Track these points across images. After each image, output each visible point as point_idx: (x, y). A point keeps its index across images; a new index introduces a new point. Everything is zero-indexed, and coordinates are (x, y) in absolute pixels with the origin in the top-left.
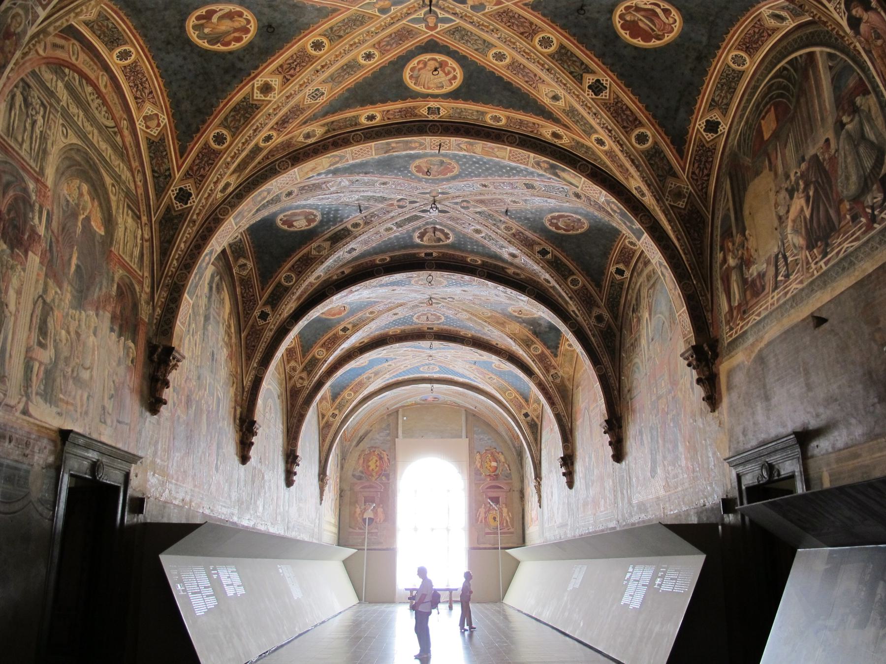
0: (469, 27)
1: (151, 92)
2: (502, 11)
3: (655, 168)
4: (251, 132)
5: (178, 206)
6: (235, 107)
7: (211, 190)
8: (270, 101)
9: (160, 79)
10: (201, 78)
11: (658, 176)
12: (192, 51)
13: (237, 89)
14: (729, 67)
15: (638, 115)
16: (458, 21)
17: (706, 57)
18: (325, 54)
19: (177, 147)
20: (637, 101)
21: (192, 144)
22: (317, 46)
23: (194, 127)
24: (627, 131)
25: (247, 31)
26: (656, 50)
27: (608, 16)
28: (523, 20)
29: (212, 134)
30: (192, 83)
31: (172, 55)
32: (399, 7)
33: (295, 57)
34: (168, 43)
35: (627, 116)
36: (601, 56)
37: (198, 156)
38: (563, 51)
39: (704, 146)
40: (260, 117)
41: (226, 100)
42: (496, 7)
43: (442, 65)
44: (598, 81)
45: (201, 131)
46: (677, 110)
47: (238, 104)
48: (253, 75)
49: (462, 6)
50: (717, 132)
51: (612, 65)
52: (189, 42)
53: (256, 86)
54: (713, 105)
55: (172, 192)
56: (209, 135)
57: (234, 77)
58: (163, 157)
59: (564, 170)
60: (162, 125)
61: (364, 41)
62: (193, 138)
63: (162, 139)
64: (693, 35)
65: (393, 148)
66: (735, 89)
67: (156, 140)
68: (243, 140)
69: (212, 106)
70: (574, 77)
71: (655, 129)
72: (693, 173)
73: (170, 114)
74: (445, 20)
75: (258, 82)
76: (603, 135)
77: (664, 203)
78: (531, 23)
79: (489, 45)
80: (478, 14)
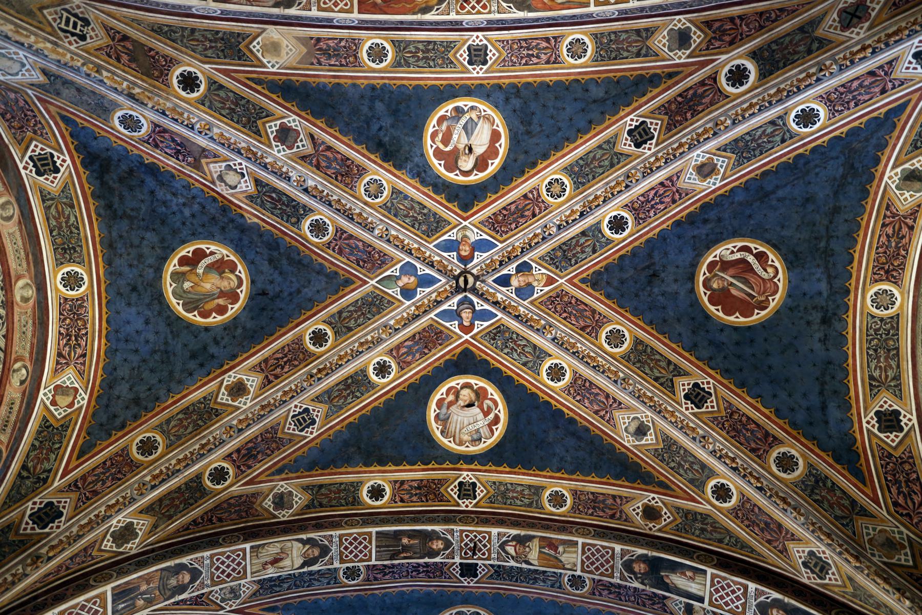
0: (514, 324)
2: (553, 294)
3: (826, 505)
4: (197, 447)
6: (188, 408)
7: (97, 516)
8: (238, 408)
9: (103, 341)
10: (157, 357)
11: (836, 518)
12: (160, 313)
13: (199, 384)
14: (873, 317)
15: (768, 428)
16: (500, 315)
17: (835, 314)
18: (327, 352)
19: (80, 442)
20: (759, 406)
21: (105, 443)
22: (319, 338)
23: (118, 422)
24: (759, 454)
25: (234, 298)
26: (764, 325)
27: (689, 285)
28: (582, 307)
29: (140, 438)
30: (144, 361)
31: (133, 310)
32: (427, 290)
33: (286, 349)
34: (134, 289)
35: (752, 432)
36: (692, 348)
37: (104, 463)
38: (640, 348)
39: (890, 456)
40: (216, 430)
41: (179, 396)
42: (547, 289)
43: (480, 394)
44: (696, 385)
45: (126, 430)
46: (824, 408)
47: (193, 404)
48: (226, 367)
49: (504, 289)
50: (901, 429)
51: (711, 358)
52: (160, 297)
53: (225, 383)
54: (875, 385)
56: (134, 439)
57: (202, 365)
58: (51, 450)
59: (674, 567)
60: (76, 406)
61: (380, 341)
62: (110, 435)
63: (65, 426)
64: (805, 286)
65: (406, 548)
66: (897, 349)
67: (56, 425)
68: (181, 457)
69: (157, 399)
70: (661, 384)
71: (802, 443)
72: (896, 504)
73: (95, 394)
74: (484, 315)
75: (230, 378)
76: (724, 475)
77: (870, 560)
78: (594, 311)
79: (540, 354)
80: (525, 303)
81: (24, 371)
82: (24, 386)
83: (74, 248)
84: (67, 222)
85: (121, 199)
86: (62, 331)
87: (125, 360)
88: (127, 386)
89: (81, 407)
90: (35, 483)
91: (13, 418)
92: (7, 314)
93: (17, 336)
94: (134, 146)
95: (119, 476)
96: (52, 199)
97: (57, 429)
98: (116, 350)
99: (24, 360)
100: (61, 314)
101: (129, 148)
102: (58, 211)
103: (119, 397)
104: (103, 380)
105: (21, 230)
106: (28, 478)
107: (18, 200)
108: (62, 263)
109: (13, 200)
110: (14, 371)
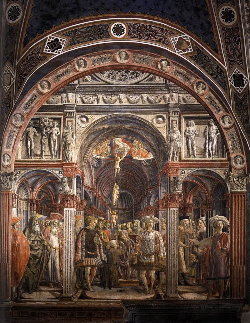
1: (162, 30)
5: (240, 90)
9: (155, 18)
21: (215, 37)
29: (220, 17)
37: (226, 42)
55: (231, 82)
58: (208, 61)
60: (189, 41)
62: (212, 32)
81: (163, 62)
82: (171, 63)
83: (100, 29)
84: (85, 33)
85: (66, 6)
86: (146, 38)
87: (169, 8)
88: (186, 11)
89: (190, 39)
90: (221, 75)
91: (185, 73)
92: (132, 70)
93: (144, 65)
94: (29, 5)
95: (237, 39)
96: (73, 40)
97: (198, 54)
98: (162, 11)
99: (158, 61)
100: (137, 37)
101: (31, 7)
102: (80, 37)
103: (191, 19)
104: (179, 24)
105: (91, 56)
106: (217, 76)
107: (76, 57)
108: (109, 35)
109: (76, 59)
110: (162, 69)
